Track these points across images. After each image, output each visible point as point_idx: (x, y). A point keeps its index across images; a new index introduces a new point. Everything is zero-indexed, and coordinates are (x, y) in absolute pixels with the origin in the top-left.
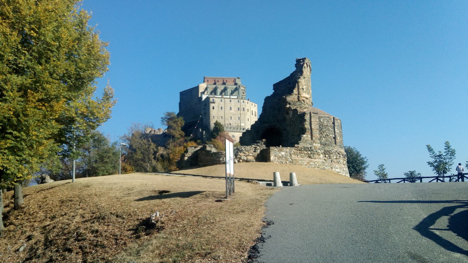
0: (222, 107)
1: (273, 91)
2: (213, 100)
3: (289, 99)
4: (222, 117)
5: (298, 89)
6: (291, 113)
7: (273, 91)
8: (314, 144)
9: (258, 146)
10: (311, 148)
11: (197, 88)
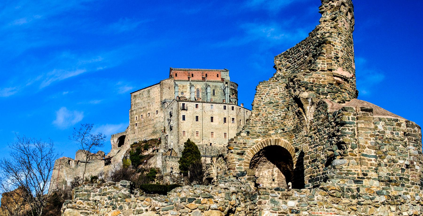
0: (197, 117)
2: (184, 104)
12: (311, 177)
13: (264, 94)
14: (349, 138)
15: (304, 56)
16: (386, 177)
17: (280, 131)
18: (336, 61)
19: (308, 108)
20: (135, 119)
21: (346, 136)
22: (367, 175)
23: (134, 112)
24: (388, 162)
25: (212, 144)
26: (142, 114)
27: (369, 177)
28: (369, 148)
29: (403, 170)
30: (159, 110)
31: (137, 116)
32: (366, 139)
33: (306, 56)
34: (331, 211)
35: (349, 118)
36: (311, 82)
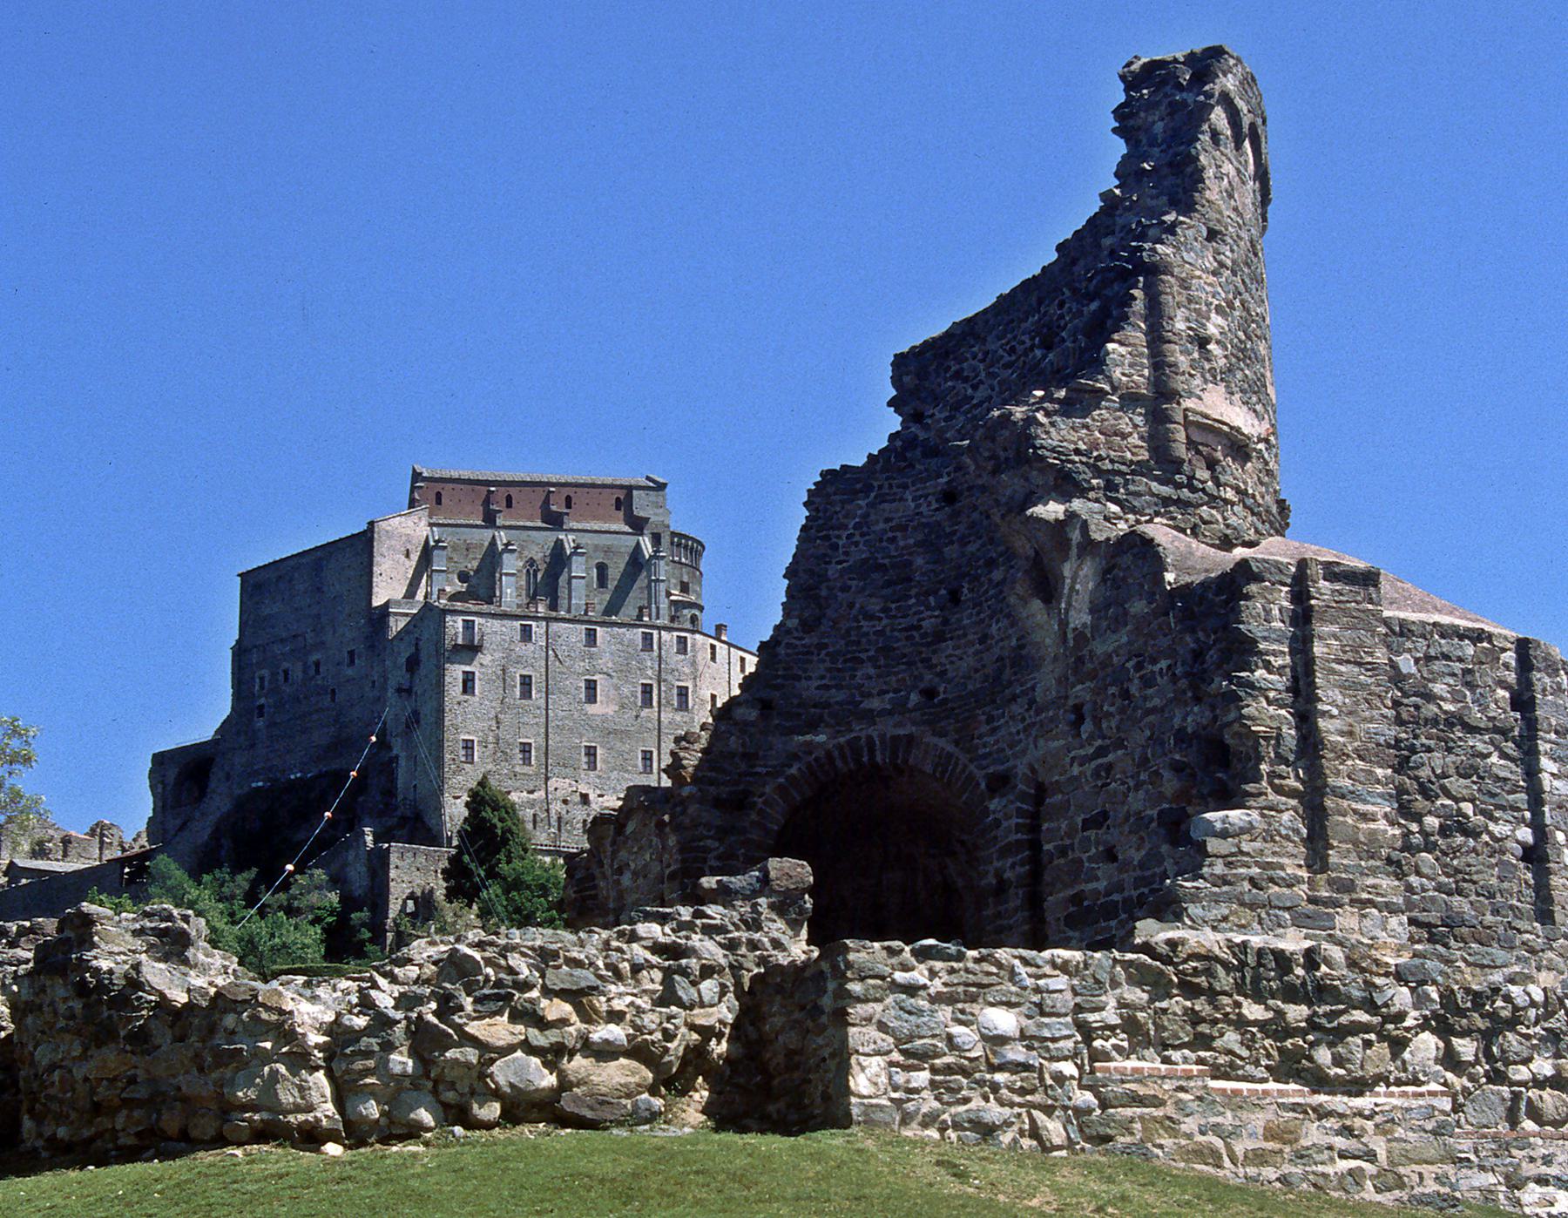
0: (526, 682)
1: (894, 423)
2: (468, 626)
3: (1060, 435)
5: (1157, 338)
6: (1080, 580)
7: (894, 423)
8: (1346, 920)
9: (709, 931)
10: (1312, 959)
11: (362, 546)
12: (1077, 899)
13: (846, 527)
15: (1032, 348)
16: (1433, 899)
17: (914, 698)
18: (1196, 355)
19: (1067, 570)
21: (1255, 698)
22: (1348, 887)
24: (1444, 831)
25: (592, 797)
26: (286, 665)
27: (1365, 896)
28: (1361, 758)
30: (360, 647)
31: (265, 672)
33: (1038, 353)
34: (1186, 1060)
35: (1268, 612)
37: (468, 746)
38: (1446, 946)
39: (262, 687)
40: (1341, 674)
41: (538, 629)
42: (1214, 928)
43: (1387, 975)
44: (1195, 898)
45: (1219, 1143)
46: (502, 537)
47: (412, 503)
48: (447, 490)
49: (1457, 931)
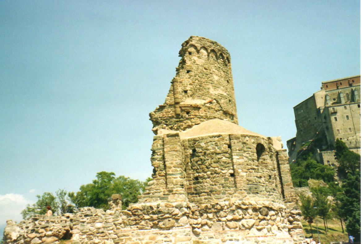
0: (347, 117)
2: (333, 109)
4: (350, 129)
14: (158, 162)
16: (209, 187)
20: (300, 127)
23: (299, 121)
24: (212, 174)
28: (174, 167)
29: (226, 179)
31: (301, 124)
32: (172, 160)
34: (134, 227)
36: (161, 116)
37: (338, 130)
38: (210, 196)
39: (301, 126)
40: (170, 153)
41: (348, 106)
42: (144, 203)
43: (173, 207)
44: (140, 198)
45: (138, 241)
46: (340, 91)
47: (321, 88)
48: (328, 85)
49: (213, 193)
